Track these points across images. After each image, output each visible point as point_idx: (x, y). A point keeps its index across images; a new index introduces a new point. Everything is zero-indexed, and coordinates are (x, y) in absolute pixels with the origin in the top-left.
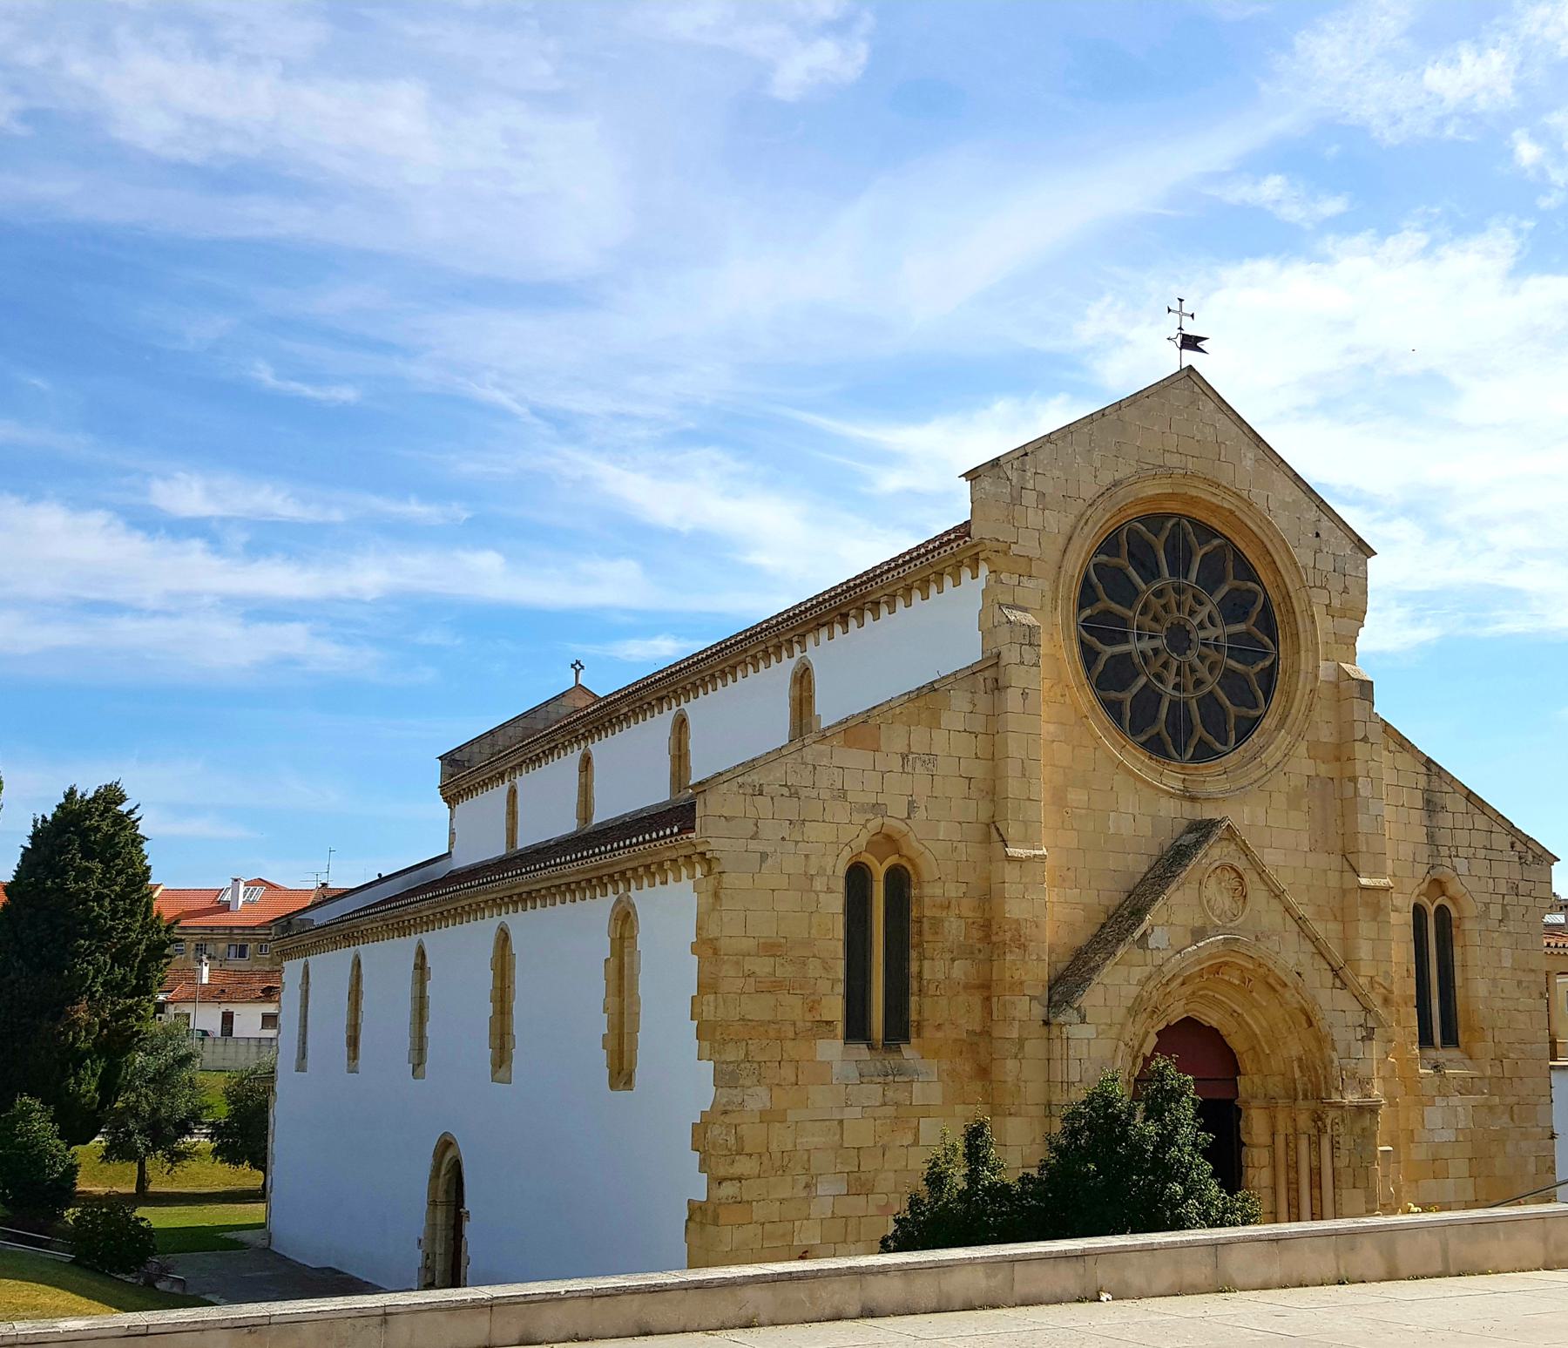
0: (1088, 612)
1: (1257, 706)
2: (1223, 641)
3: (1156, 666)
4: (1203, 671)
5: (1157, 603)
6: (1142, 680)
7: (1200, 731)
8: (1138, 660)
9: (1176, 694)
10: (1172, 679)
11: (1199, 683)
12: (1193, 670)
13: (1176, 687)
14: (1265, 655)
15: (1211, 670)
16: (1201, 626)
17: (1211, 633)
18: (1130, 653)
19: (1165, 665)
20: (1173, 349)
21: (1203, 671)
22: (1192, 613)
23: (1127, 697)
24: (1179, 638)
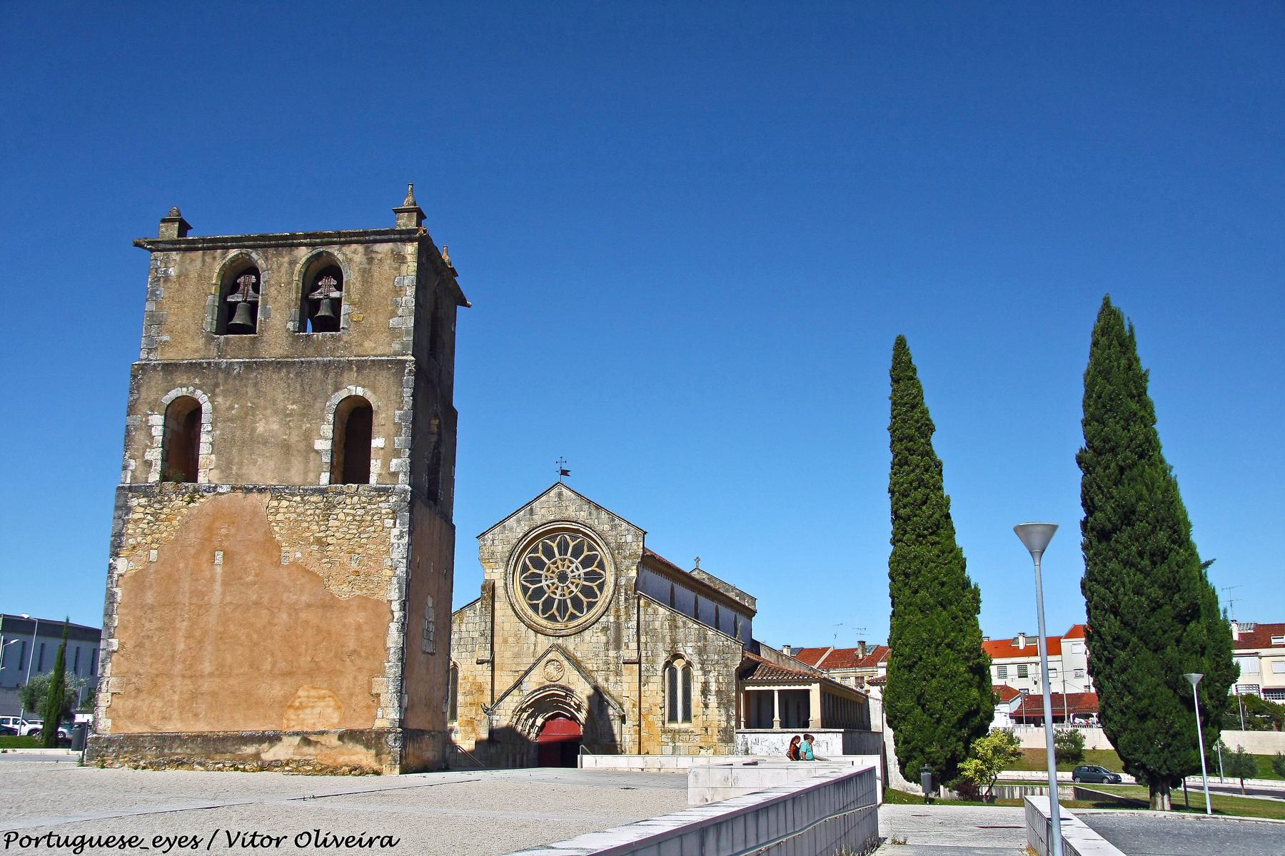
0: (525, 575)
1: (597, 597)
2: (582, 575)
3: (552, 588)
4: (573, 588)
5: (553, 567)
6: (546, 595)
7: (571, 609)
8: (546, 588)
9: (561, 598)
10: (558, 592)
11: (572, 592)
12: (568, 588)
13: (561, 596)
14: (601, 578)
15: (577, 587)
16: (572, 571)
17: (577, 573)
18: (542, 586)
19: (557, 588)
20: (558, 475)
21: (573, 588)
22: (569, 567)
23: (540, 602)
24: (563, 577)
